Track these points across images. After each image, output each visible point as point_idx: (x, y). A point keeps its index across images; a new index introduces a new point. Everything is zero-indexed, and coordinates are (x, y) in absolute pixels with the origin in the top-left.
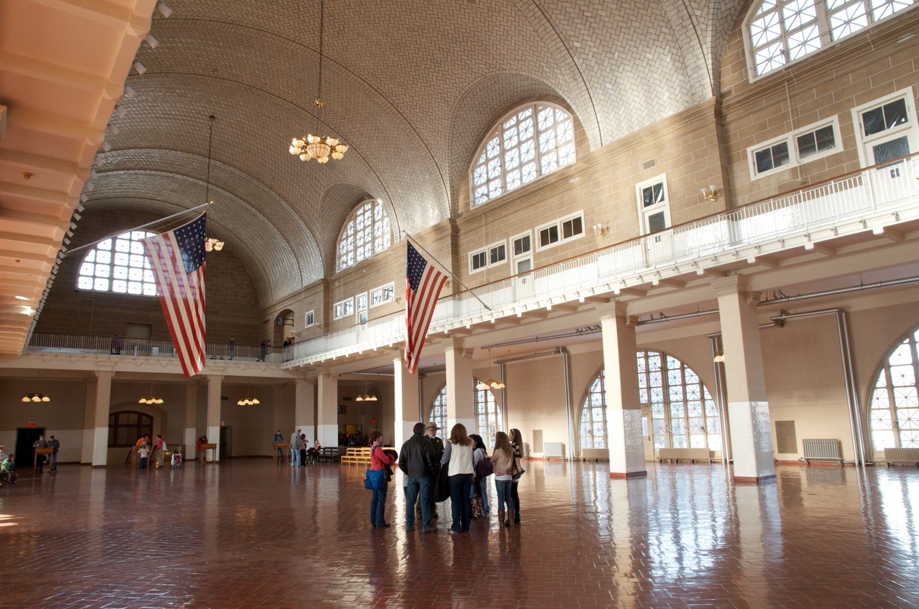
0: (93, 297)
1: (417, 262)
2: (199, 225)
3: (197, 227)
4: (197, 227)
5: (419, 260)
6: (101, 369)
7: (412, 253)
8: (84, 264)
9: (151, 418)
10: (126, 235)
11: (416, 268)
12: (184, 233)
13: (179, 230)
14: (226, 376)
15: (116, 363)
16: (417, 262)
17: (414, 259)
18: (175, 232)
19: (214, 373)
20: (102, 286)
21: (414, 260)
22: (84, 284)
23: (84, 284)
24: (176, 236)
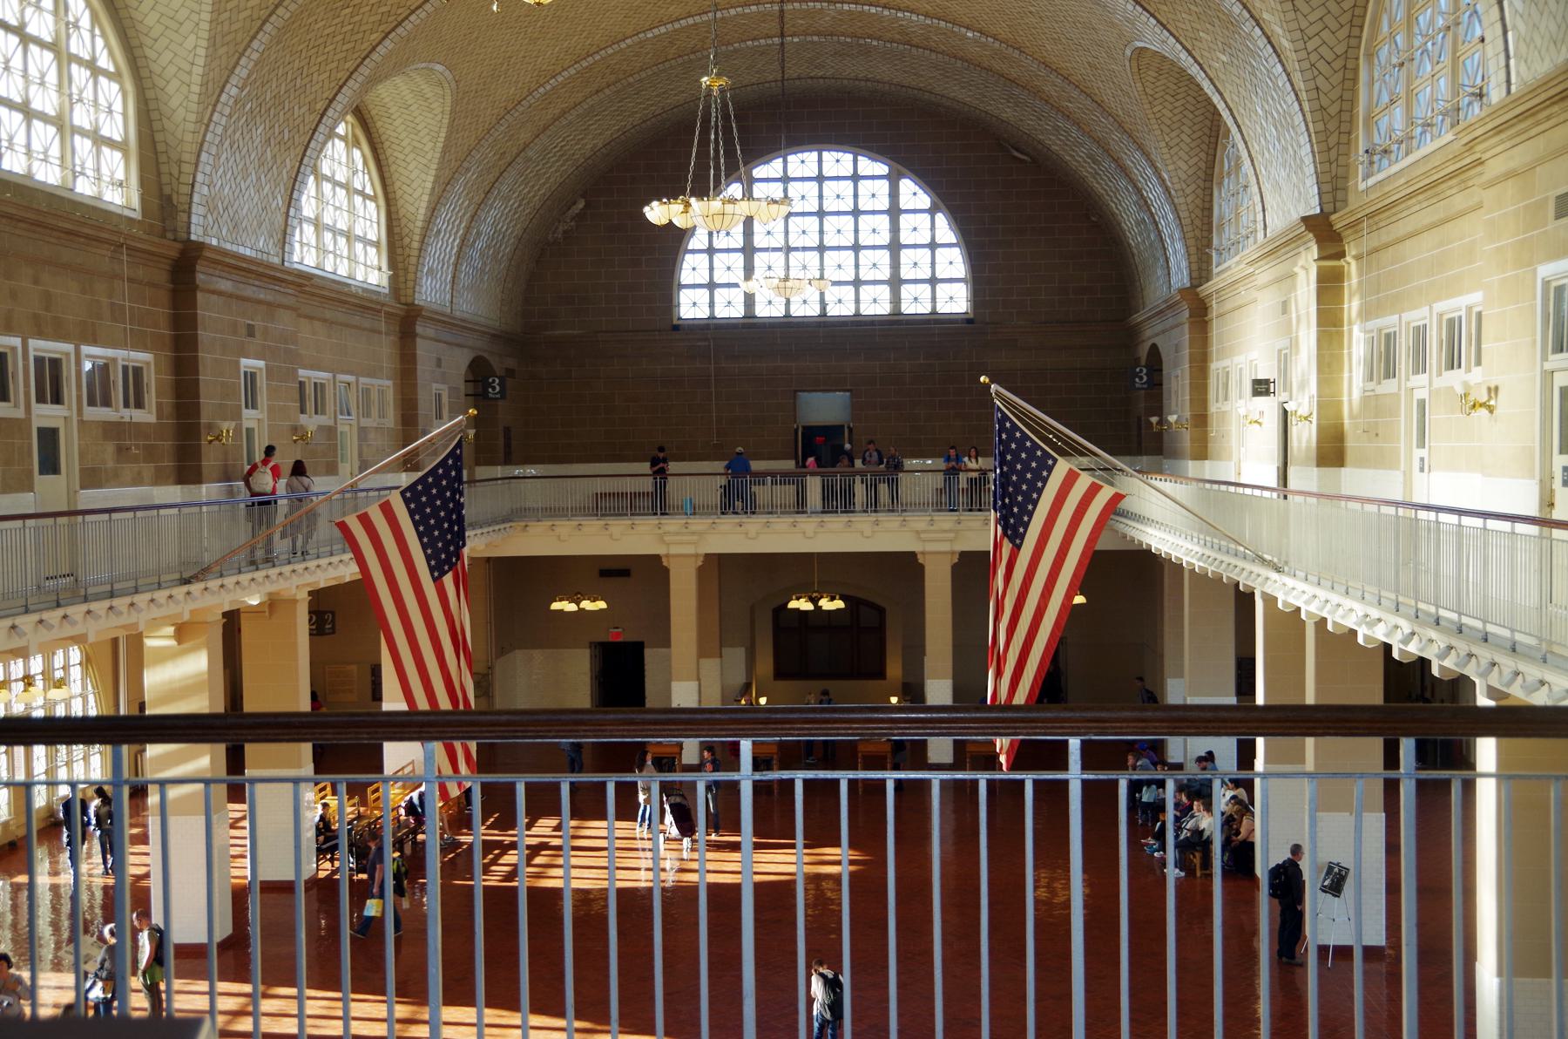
0: (712, 329)
1: (1026, 464)
2: (430, 486)
3: (446, 475)
4: (446, 475)
5: (1032, 456)
6: (674, 550)
7: (1011, 438)
8: (688, 257)
9: (881, 611)
10: (773, 168)
11: (1022, 479)
12: (421, 494)
13: (412, 487)
14: (963, 554)
15: (700, 534)
16: (1026, 464)
17: (1016, 454)
18: (403, 493)
19: (930, 547)
20: (730, 307)
21: (1016, 458)
22: (692, 306)
23: (692, 306)
24: (407, 502)
